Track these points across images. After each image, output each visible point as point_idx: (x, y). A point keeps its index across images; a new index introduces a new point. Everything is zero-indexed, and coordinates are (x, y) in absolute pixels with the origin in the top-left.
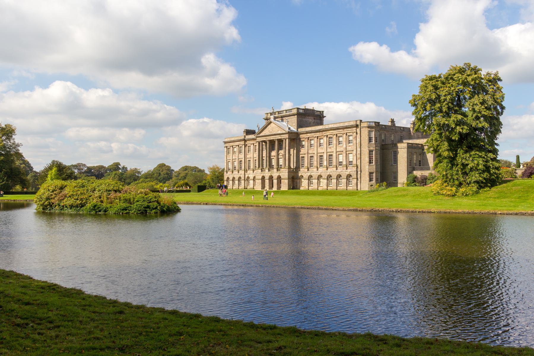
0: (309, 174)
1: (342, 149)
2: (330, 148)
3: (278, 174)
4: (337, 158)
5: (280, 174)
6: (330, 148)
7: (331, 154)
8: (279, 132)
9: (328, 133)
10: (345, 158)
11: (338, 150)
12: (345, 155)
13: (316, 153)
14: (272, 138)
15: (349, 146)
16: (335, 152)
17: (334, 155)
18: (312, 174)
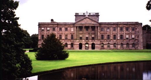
0: (107, 43)
1: (128, 33)
2: (121, 32)
3: (92, 42)
4: (126, 36)
5: (94, 43)
6: (121, 32)
7: (122, 34)
8: (93, 23)
9: (120, 26)
10: (130, 37)
11: (126, 33)
12: (130, 35)
13: (111, 33)
14: (87, 25)
15: (133, 32)
16: (125, 34)
17: (125, 35)
18: (110, 43)
